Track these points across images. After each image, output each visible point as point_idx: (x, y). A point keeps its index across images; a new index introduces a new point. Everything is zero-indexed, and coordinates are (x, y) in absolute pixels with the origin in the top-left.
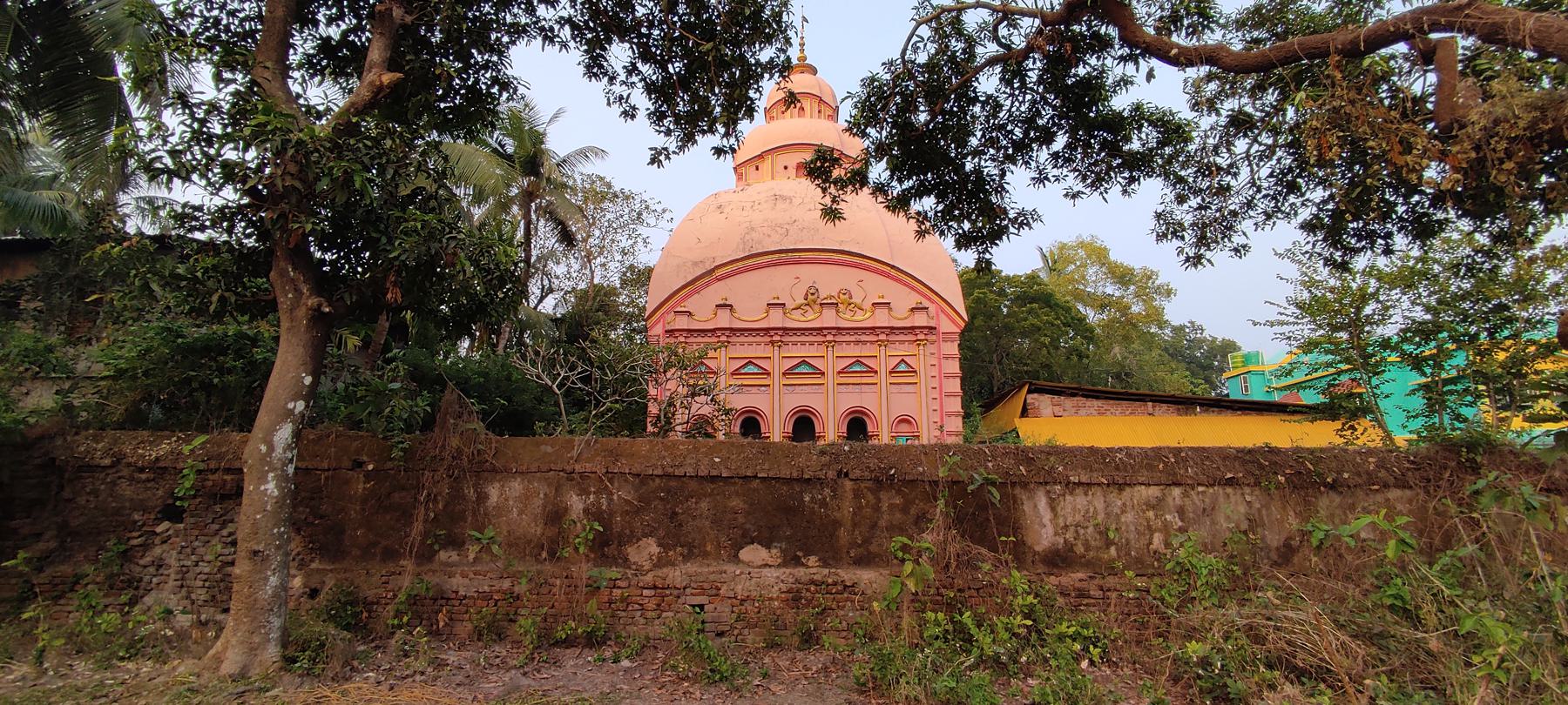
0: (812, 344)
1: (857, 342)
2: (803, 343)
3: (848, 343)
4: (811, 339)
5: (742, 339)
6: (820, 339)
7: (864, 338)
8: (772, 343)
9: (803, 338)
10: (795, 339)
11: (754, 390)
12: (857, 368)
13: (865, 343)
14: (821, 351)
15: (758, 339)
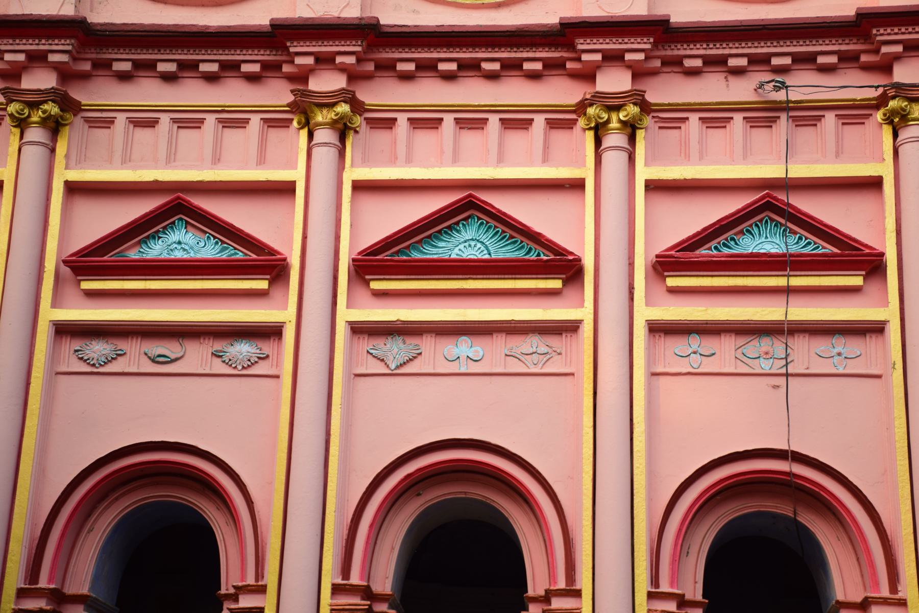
0: (516, 121)
1: (764, 114)
2: (471, 121)
3: (716, 116)
4: (515, 93)
5: (148, 93)
6: (562, 92)
7: (805, 86)
8: (304, 109)
9: (472, 93)
10: (429, 93)
11: (196, 356)
12: (766, 242)
13: (806, 114)
14: (573, 156)
15: (234, 94)
